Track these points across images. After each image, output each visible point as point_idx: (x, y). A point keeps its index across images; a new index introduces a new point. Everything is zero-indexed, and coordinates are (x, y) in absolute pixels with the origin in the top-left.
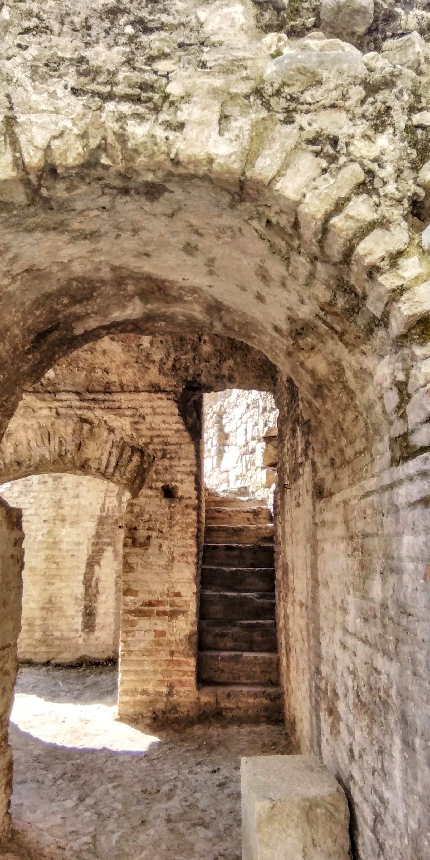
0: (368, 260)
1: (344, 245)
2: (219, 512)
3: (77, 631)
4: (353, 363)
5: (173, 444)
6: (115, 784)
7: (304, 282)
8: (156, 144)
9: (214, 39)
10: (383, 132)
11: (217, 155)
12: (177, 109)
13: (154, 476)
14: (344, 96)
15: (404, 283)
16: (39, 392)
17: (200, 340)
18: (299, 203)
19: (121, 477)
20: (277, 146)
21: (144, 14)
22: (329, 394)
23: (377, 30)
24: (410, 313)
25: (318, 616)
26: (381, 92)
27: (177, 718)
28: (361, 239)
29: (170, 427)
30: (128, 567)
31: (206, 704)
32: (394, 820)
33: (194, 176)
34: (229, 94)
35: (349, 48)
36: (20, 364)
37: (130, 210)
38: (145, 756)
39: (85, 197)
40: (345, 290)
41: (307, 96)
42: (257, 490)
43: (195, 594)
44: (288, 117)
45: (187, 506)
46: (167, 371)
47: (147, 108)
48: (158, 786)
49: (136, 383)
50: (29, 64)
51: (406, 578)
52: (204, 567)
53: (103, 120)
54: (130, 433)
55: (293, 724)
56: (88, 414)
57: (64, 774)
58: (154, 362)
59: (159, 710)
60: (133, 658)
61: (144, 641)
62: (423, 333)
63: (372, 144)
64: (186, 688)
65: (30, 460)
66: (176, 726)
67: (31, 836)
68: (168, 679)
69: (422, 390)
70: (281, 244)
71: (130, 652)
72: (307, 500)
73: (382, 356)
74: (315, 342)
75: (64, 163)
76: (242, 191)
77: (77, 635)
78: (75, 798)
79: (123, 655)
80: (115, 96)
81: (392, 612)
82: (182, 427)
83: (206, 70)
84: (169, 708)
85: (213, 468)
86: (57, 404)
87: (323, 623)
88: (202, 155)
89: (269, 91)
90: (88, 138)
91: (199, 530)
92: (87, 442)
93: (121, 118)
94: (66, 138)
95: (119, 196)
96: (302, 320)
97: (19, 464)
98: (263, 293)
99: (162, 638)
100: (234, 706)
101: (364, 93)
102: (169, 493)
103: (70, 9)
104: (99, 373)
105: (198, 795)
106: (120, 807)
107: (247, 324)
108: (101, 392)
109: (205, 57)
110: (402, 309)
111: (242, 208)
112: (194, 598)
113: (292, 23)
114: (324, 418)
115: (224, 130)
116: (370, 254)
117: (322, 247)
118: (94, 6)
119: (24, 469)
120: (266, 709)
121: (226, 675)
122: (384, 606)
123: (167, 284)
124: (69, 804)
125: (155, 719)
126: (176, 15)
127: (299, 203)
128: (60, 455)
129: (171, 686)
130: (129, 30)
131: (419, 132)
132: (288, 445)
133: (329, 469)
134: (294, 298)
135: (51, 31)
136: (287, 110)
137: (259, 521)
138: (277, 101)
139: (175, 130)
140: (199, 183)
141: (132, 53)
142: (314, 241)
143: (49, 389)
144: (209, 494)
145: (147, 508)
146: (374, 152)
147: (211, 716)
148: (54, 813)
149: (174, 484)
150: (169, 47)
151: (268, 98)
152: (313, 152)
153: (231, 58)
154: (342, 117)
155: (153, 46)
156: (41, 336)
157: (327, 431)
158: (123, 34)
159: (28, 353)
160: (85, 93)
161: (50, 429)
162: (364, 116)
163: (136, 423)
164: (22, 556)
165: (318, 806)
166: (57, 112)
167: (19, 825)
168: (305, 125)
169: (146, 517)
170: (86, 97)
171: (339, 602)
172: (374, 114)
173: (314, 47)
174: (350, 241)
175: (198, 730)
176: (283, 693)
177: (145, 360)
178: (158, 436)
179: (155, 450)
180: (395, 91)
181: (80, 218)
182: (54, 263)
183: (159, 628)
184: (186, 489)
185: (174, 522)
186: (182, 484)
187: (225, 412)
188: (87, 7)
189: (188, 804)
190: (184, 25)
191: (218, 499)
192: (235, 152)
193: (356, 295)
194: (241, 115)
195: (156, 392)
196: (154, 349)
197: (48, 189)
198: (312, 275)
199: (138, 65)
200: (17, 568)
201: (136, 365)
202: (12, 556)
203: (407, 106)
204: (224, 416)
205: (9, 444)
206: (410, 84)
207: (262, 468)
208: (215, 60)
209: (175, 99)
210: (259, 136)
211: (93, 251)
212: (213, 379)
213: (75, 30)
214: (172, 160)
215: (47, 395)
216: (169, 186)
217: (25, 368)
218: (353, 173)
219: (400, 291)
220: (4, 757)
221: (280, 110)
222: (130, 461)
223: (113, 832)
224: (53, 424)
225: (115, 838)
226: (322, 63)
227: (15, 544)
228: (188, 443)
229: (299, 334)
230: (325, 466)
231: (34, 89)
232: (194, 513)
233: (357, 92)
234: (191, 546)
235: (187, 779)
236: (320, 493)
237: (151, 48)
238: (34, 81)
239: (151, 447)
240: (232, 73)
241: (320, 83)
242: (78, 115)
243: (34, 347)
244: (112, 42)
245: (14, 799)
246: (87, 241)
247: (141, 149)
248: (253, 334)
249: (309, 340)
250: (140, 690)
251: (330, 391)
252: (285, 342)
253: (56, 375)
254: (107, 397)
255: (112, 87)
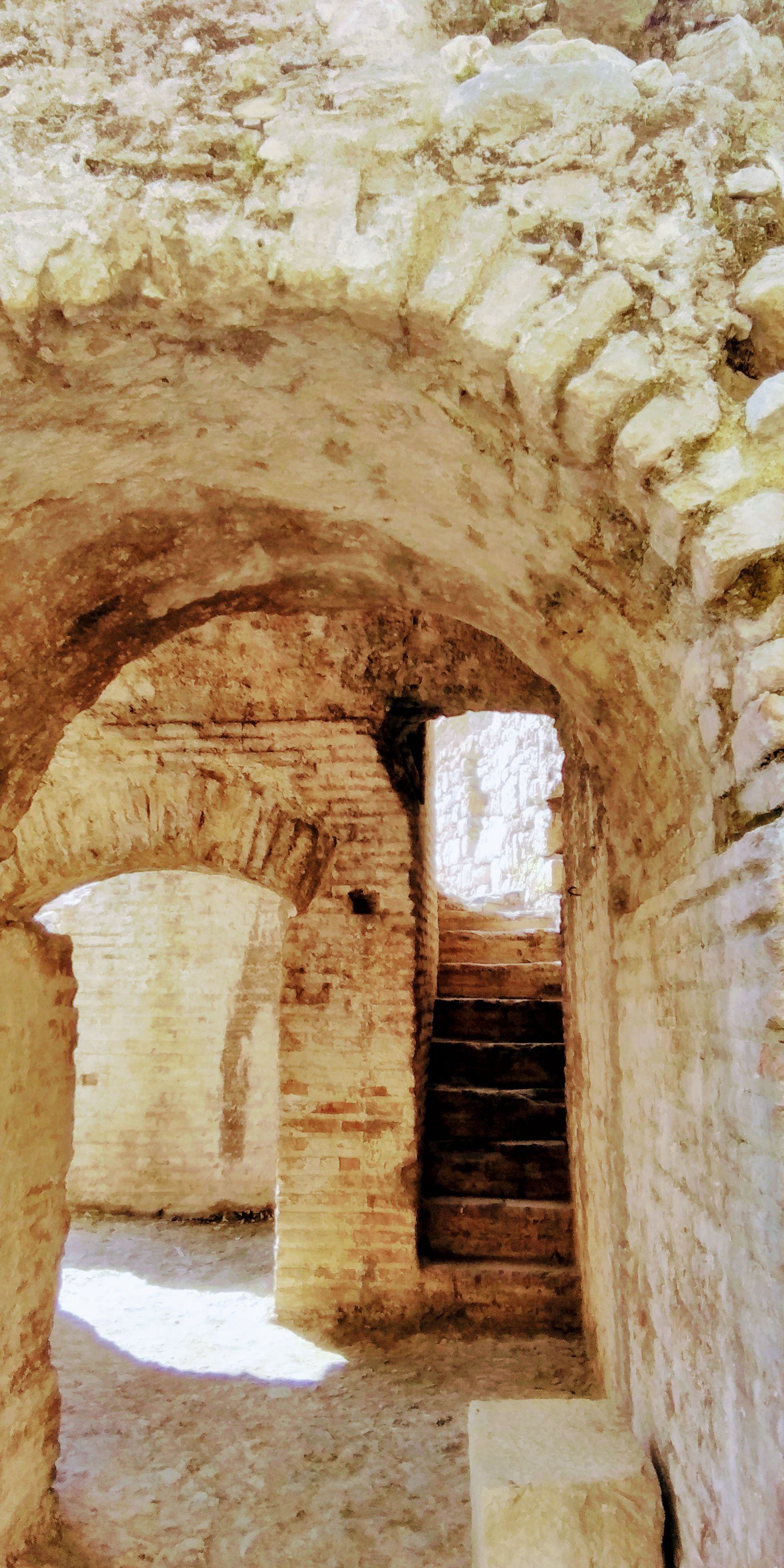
0: (642, 458)
1: (597, 431)
2: (466, 939)
3: (210, 1155)
4: (648, 656)
5: (368, 815)
6: (257, 1440)
7: (542, 506)
8: (240, 256)
9: (347, 53)
10: (668, 209)
11: (352, 269)
12: (279, 187)
13: (335, 874)
14: (593, 145)
15: (711, 498)
16: (128, 725)
17: (415, 621)
18: (507, 354)
19: (277, 875)
20: (465, 247)
21: (218, 15)
22: (620, 717)
23: (665, 18)
24: (724, 557)
25: (621, 1136)
26: (665, 134)
27: (381, 1321)
28: (628, 418)
29: (362, 783)
30: (289, 1041)
31: (435, 1295)
32: (729, 1535)
33: (312, 314)
34: (376, 154)
35: (609, 57)
36: (50, 673)
37: (213, 382)
38: (319, 1391)
39: (125, 361)
40: (614, 518)
41: (523, 151)
42: (538, 899)
43: (414, 1091)
44: (488, 191)
45: (395, 929)
46: (356, 681)
47: (224, 189)
48: (336, 1446)
49: (300, 703)
50: (10, 120)
51: (736, 1067)
52: (435, 1040)
53: (142, 215)
54: (289, 795)
55: (594, 1335)
56: (214, 763)
57: (168, 1419)
58: (331, 665)
59: (348, 1305)
60: (301, 1207)
61: (319, 1176)
62: (753, 595)
63: (647, 235)
64: (398, 1266)
65: (115, 847)
66: (380, 1335)
67: (94, 1534)
68: (364, 1247)
69: (752, 704)
70: (490, 432)
71: (295, 1197)
72: (602, 915)
73: (690, 642)
74: (581, 618)
75: (76, 299)
76: (407, 337)
77: (212, 1164)
78: (182, 1465)
79: (283, 1203)
80: (165, 169)
81: (718, 1134)
82: (384, 783)
83: (333, 112)
84: (368, 1299)
85: (461, 859)
86: (159, 745)
87: (627, 1150)
88: (325, 272)
89: (450, 144)
90: (117, 250)
91: (420, 973)
92: (214, 813)
93: (176, 209)
94: (76, 250)
95: (190, 356)
96: (552, 577)
97: (96, 854)
98: (479, 529)
99: (352, 1173)
100: (488, 1301)
101: (631, 138)
102: (362, 904)
103: (84, 15)
104: (234, 688)
105: (406, 1466)
106: (258, 1482)
107: (463, 588)
108: (237, 721)
109: (330, 88)
110: (708, 550)
111: (413, 369)
112: (410, 1099)
113: (502, 15)
114: (618, 762)
115: (365, 223)
116: (646, 446)
117: (560, 437)
118: (127, 6)
119: (104, 863)
120: (548, 1306)
121: (473, 1242)
122: (708, 1123)
123: (308, 518)
124: (170, 1476)
125: (342, 1321)
126: (278, 14)
127: (507, 354)
128: (168, 838)
129: (370, 1261)
130: (192, 46)
131: (741, 206)
132: (575, 814)
133: (634, 858)
134: (533, 538)
135: (50, 58)
136: (486, 179)
137: (539, 955)
138: (467, 163)
139: (276, 228)
140: (327, 325)
141: (197, 88)
142: (544, 424)
143: (145, 718)
144: (447, 907)
145: (323, 933)
146: (651, 250)
147: (444, 1318)
148: (141, 1492)
149: (371, 888)
150: (263, 73)
151: (448, 157)
152: (534, 255)
153: (379, 87)
154: (591, 185)
155: (234, 74)
156: (87, 621)
157: (623, 787)
158: (180, 56)
159: (63, 652)
160: (111, 167)
161: (149, 792)
162: (632, 182)
163: (301, 777)
164: (73, 1024)
165: (602, 1498)
166: (60, 207)
167: (73, 1514)
168: (519, 206)
169: (321, 949)
170: (113, 175)
171: (647, 1110)
172: (652, 177)
173: (539, 57)
174: (608, 421)
175: (419, 1343)
176: (578, 1279)
177: (316, 662)
178: (341, 800)
179: (335, 826)
180: (690, 130)
181: (122, 402)
182: (90, 485)
183: (348, 1153)
184: (394, 896)
185: (372, 959)
186: (385, 887)
187: (481, 755)
188: (116, 10)
189: (385, 1482)
190: (291, 30)
191: (463, 915)
192: (387, 264)
193: (634, 527)
194: (398, 193)
195: (336, 719)
196: (332, 640)
197: (54, 348)
198: (553, 491)
199: (207, 110)
200: (63, 1044)
201: (299, 671)
202: (52, 1023)
203: (716, 158)
204: (480, 762)
205: (77, 819)
206: (721, 117)
207: (547, 857)
208: (350, 93)
209: (274, 169)
210: (432, 230)
211: (160, 462)
212: (441, 693)
213: (94, 54)
214: (271, 283)
215: (141, 731)
216: (275, 333)
217: (61, 680)
218: (615, 293)
219: (704, 514)
220: (41, 1388)
221: (472, 180)
222: (292, 846)
223: (244, 1533)
224: (153, 782)
225: (245, 1542)
226: (550, 85)
227: (58, 1001)
228: (397, 813)
229: (554, 604)
230: (628, 853)
231: (19, 166)
232: (409, 941)
233: (620, 137)
234: (404, 1002)
235: (389, 1436)
236: (621, 903)
237: (230, 78)
238: (19, 151)
239: (328, 820)
240: (381, 115)
241: (547, 123)
242: (98, 209)
243: (73, 642)
244: (159, 71)
245: (69, 1466)
246: (145, 444)
247: (214, 266)
248: (479, 608)
249: (571, 614)
250: (314, 1267)
251: (619, 710)
252: (533, 620)
253: (158, 692)
254: (249, 730)
255: (159, 154)
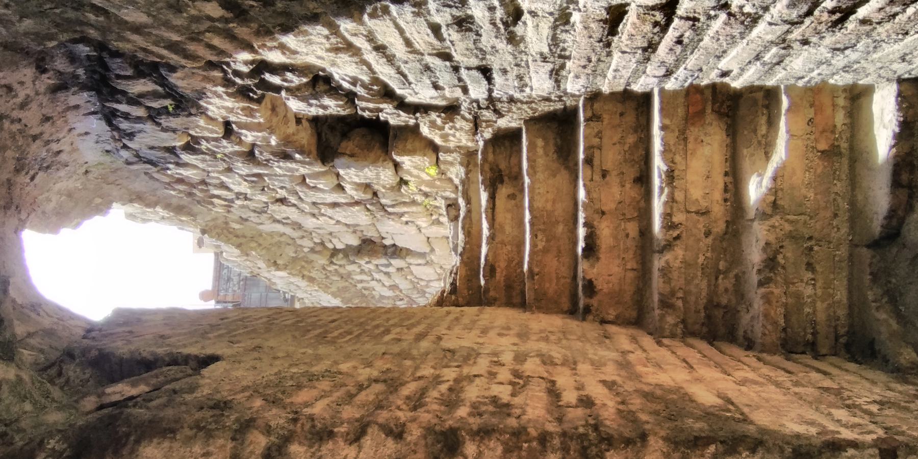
85: (427, 263)
204: (330, 246)
207: (397, 166)
